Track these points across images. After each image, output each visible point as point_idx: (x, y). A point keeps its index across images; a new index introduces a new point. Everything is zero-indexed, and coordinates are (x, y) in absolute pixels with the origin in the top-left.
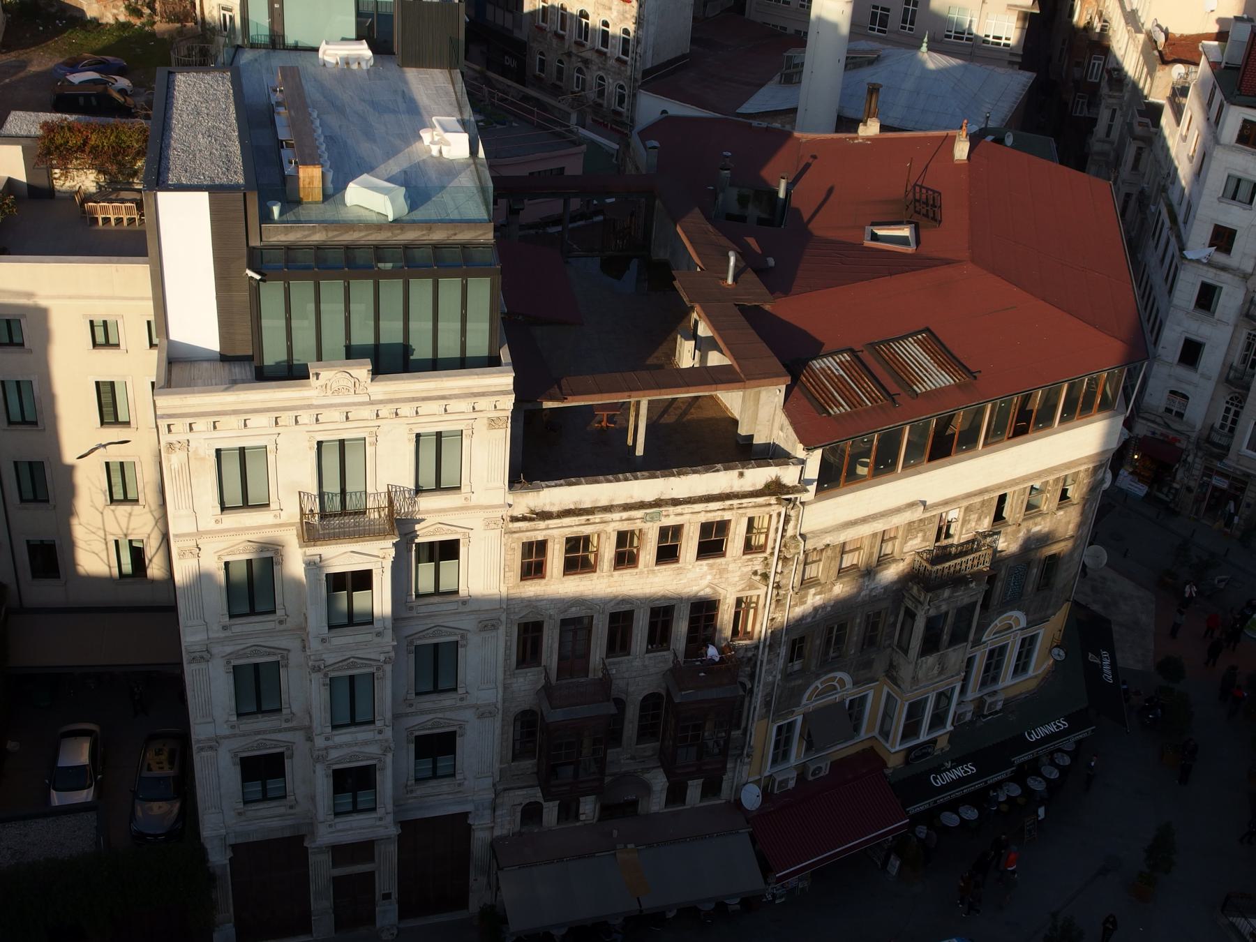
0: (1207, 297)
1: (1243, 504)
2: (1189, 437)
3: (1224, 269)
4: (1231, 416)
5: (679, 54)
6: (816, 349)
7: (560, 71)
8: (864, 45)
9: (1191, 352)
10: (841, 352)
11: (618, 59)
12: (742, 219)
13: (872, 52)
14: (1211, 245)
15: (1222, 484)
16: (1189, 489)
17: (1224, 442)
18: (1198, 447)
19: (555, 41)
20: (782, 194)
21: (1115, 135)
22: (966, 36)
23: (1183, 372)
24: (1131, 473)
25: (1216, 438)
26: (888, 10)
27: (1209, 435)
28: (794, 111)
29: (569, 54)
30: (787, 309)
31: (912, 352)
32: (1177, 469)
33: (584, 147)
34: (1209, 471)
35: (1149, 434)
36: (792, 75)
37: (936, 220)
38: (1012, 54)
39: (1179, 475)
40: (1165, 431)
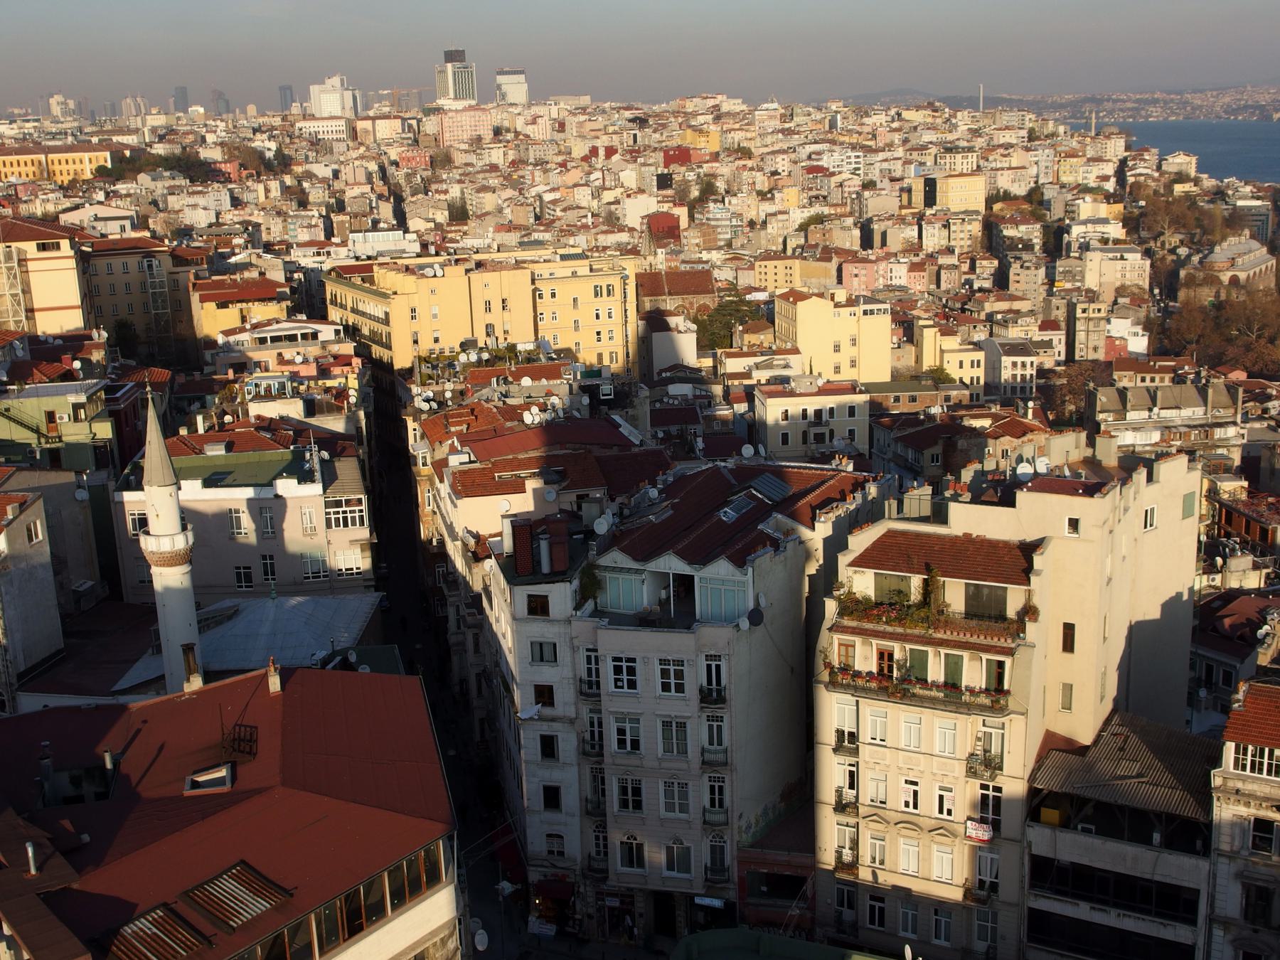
0: (548, 747)
1: (637, 915)
2: (575, 870)
3: (553, 720)
4: (601, 842)
5: (53, 650)
6: (128, 912)
8: (228, 603)
9: (552, 797)
10: (153, 910)
12: (79, 799)
13: (230, 608)
14: (537, 703)
15: (614, 903)
16: (590, 917)
17: (602, 866)
18: (584, 876)
20: (109, 765)
22: (322, 574)
23: (550, 815)
24: (538, 918)
25: (595, 865)
26: (249, 568)
27: (590, 866)
28: (162, 677)
30: (97, 882)
31: (229, 888)
32: (574, 902)
34: (600, 895)
35: (542, 878)
37: (252, 753)
38: (365, 580)
39: (578, 907)
40: (553, 870)
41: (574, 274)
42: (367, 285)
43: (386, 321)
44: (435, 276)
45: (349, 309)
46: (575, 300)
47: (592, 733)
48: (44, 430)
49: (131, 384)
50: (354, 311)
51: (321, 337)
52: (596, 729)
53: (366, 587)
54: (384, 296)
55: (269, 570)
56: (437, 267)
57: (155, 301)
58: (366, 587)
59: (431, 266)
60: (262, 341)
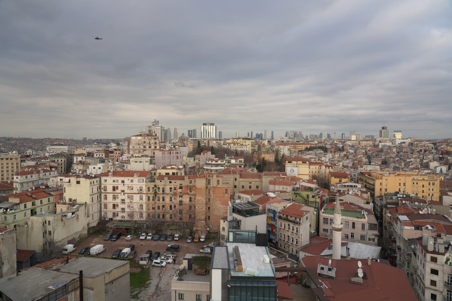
5: (307, 244)
7: (284, 247)
8: (344, 242)
11: (296, 245)
19: (283, 242)
21: (402, 260)
29: (286, 244)
33: (290, 262)
36: (330, 248)
41: (424, 179)
42: (369, 177)
43: (374, 185)
45: (364, 181)
46: (423, 185)
47: (448, 297)
48: (306, 198)
49: (322, 192)
50: (365, 182)
51: (358, 187)
52: (449, 296)
53: (375, 245)
54: (374, 180)
55: (352, 236)
56: (387, 174)
57: (321, 175)
58: (375, 245)
59: (386, 174)
60: (345, 186)
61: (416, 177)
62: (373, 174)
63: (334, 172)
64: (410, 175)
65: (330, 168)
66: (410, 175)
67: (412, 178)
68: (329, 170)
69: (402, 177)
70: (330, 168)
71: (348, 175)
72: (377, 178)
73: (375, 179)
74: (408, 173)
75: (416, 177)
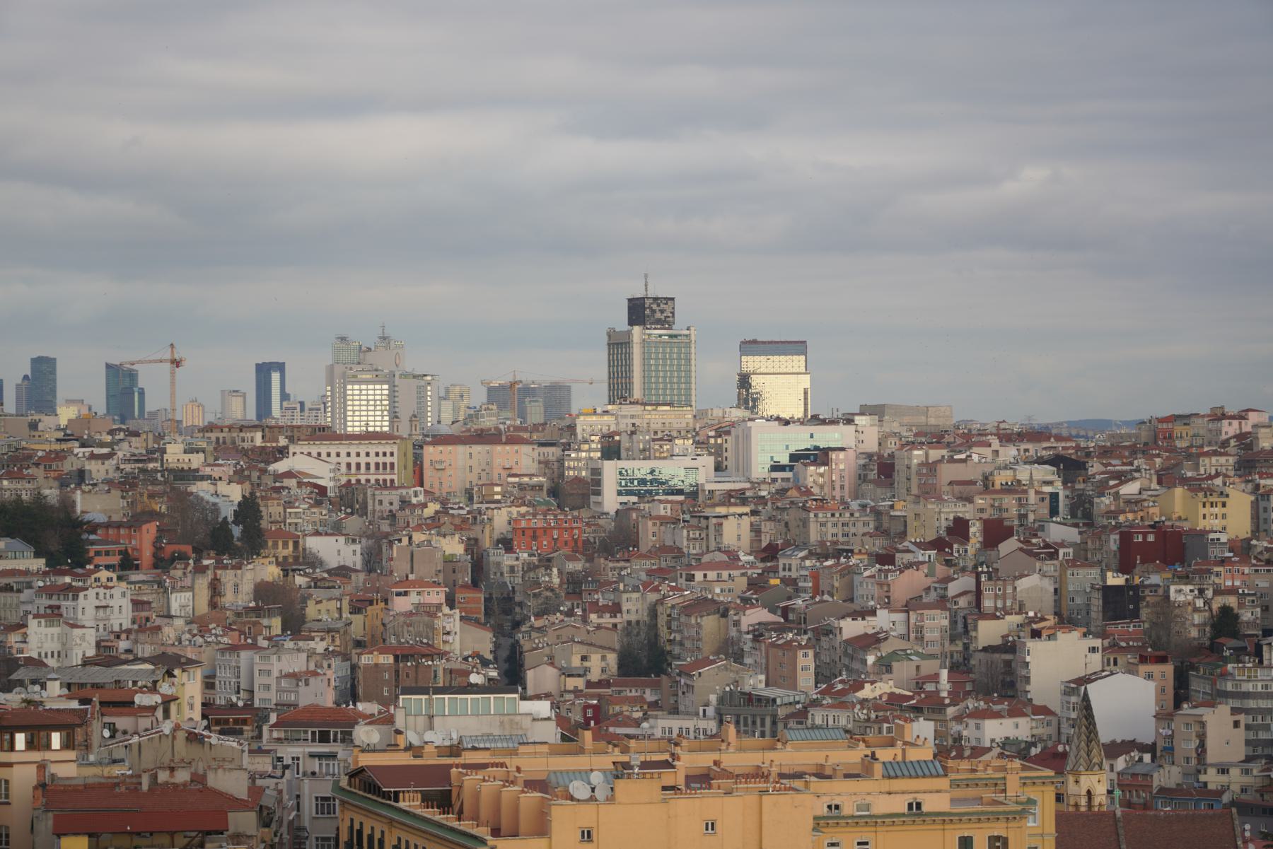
41: (915, 807)
42: (434, 814)
44: (592, 799)
56: (596, 778)
59: (584, 775)
61: (848, 796)
62: (471, 780)
63: (88, 788)
64: (798, 776)
65: (56, 740)
66: (798, 776)
67: (813, 802)
68: (42, 766)
69: (728, 799)
70: (56, 740)
71: (238, 804)
72: (505, 824)
73: (483, 832)
74: (788, 756)
75: (848, 796)
